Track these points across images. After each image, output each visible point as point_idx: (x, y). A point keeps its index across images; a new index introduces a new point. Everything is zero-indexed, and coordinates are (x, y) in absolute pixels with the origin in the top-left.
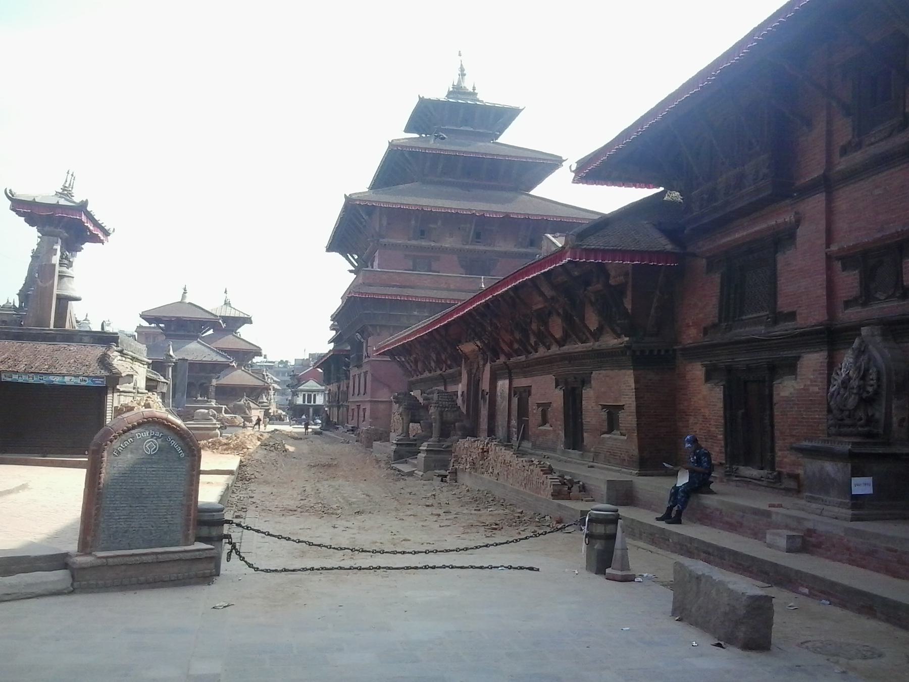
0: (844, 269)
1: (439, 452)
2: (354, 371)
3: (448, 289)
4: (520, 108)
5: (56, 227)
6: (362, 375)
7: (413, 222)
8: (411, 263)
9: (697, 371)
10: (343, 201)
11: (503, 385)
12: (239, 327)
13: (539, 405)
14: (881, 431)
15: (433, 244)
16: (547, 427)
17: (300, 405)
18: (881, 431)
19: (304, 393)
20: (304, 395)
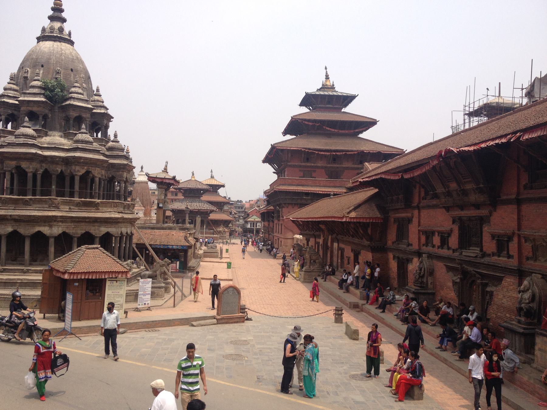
0: (423, 234)
1: (310, 272)
2: (276, 222)
3: (320, 186)
4: (356, 95)
5: (163, 185)
6: (280, 224)
7: (303, 155)
8: (302, 174)
9: (391, 256)
10: (269, 147)
11: (335, 245)
12: (218, 189)
13: (347, 257)
14: (425, 286)
15: (313, 165)
16: (349, 266)
17: (249, 228)
18: (425, 286)
19: (250, 222)
20: (251, 223)
